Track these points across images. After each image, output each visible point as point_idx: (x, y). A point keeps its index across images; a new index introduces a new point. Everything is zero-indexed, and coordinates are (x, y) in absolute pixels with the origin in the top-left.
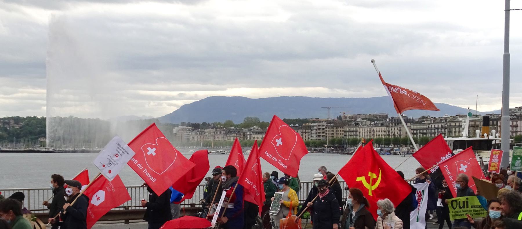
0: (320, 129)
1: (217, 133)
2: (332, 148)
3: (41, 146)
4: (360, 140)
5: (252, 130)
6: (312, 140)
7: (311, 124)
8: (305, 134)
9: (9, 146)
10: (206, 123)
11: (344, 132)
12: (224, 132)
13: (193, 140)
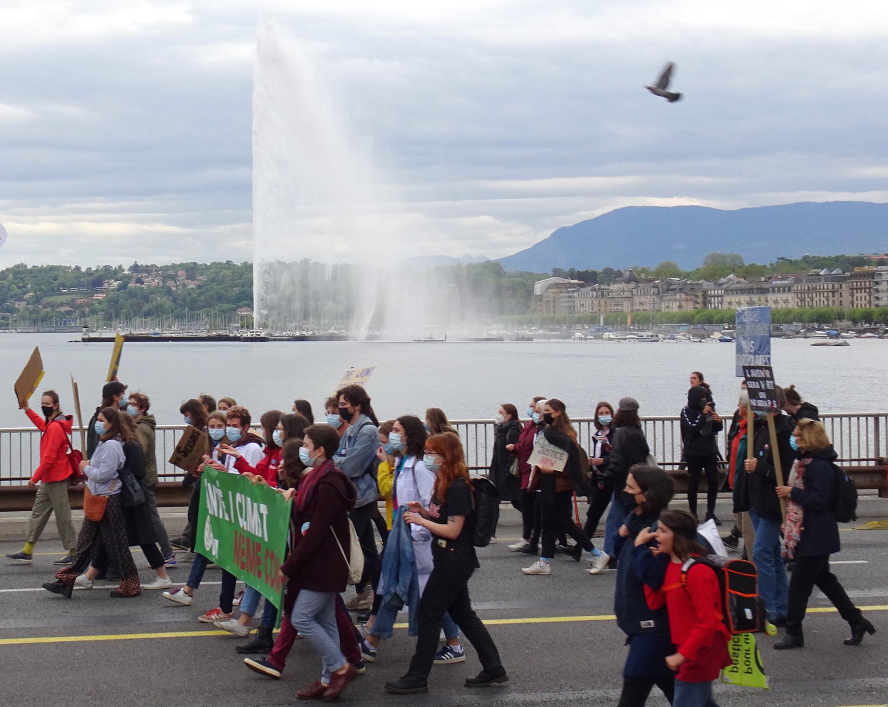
1: (642, 294)
3: (242, 327)
5: (723, 284)
6: (877, 306)
7: (876, 269)
8: (861, 292)
9: (175, 328)
10: (612, 270)
12: (656, 291)
13: (581, 309)
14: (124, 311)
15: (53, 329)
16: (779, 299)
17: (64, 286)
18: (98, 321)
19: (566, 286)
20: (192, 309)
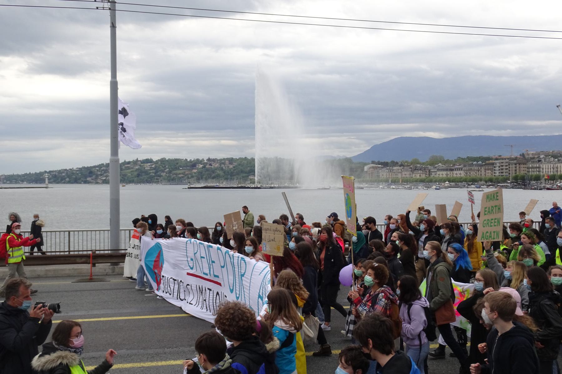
0: (502, 166)
2: (515, 184)
3: (251, 183)
4: (544, 176)
6: (495, 176)
11: (527, 168)
12: (411, 170)
14: (204, 176)
15: (176, 184)
16: (458, 173)
17: (181, 167)
18: (194, 180)
19: (376, 168)
20: (231, 176)
